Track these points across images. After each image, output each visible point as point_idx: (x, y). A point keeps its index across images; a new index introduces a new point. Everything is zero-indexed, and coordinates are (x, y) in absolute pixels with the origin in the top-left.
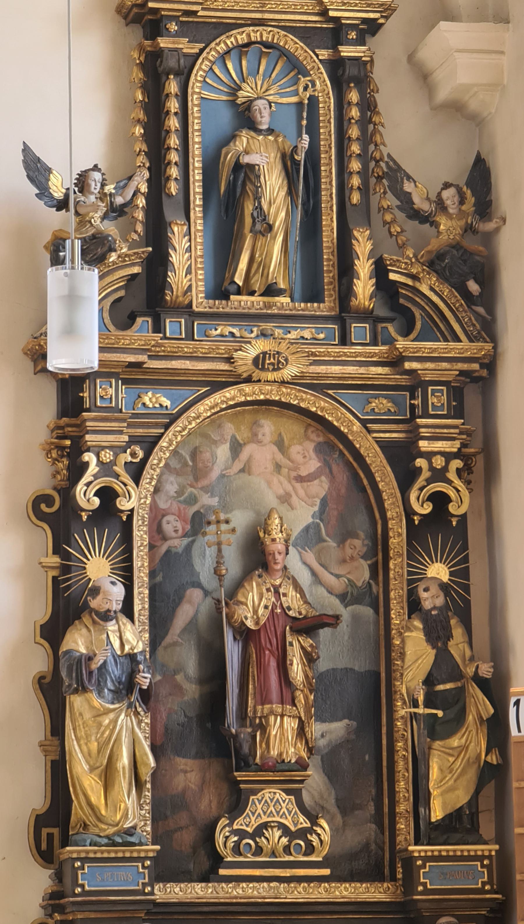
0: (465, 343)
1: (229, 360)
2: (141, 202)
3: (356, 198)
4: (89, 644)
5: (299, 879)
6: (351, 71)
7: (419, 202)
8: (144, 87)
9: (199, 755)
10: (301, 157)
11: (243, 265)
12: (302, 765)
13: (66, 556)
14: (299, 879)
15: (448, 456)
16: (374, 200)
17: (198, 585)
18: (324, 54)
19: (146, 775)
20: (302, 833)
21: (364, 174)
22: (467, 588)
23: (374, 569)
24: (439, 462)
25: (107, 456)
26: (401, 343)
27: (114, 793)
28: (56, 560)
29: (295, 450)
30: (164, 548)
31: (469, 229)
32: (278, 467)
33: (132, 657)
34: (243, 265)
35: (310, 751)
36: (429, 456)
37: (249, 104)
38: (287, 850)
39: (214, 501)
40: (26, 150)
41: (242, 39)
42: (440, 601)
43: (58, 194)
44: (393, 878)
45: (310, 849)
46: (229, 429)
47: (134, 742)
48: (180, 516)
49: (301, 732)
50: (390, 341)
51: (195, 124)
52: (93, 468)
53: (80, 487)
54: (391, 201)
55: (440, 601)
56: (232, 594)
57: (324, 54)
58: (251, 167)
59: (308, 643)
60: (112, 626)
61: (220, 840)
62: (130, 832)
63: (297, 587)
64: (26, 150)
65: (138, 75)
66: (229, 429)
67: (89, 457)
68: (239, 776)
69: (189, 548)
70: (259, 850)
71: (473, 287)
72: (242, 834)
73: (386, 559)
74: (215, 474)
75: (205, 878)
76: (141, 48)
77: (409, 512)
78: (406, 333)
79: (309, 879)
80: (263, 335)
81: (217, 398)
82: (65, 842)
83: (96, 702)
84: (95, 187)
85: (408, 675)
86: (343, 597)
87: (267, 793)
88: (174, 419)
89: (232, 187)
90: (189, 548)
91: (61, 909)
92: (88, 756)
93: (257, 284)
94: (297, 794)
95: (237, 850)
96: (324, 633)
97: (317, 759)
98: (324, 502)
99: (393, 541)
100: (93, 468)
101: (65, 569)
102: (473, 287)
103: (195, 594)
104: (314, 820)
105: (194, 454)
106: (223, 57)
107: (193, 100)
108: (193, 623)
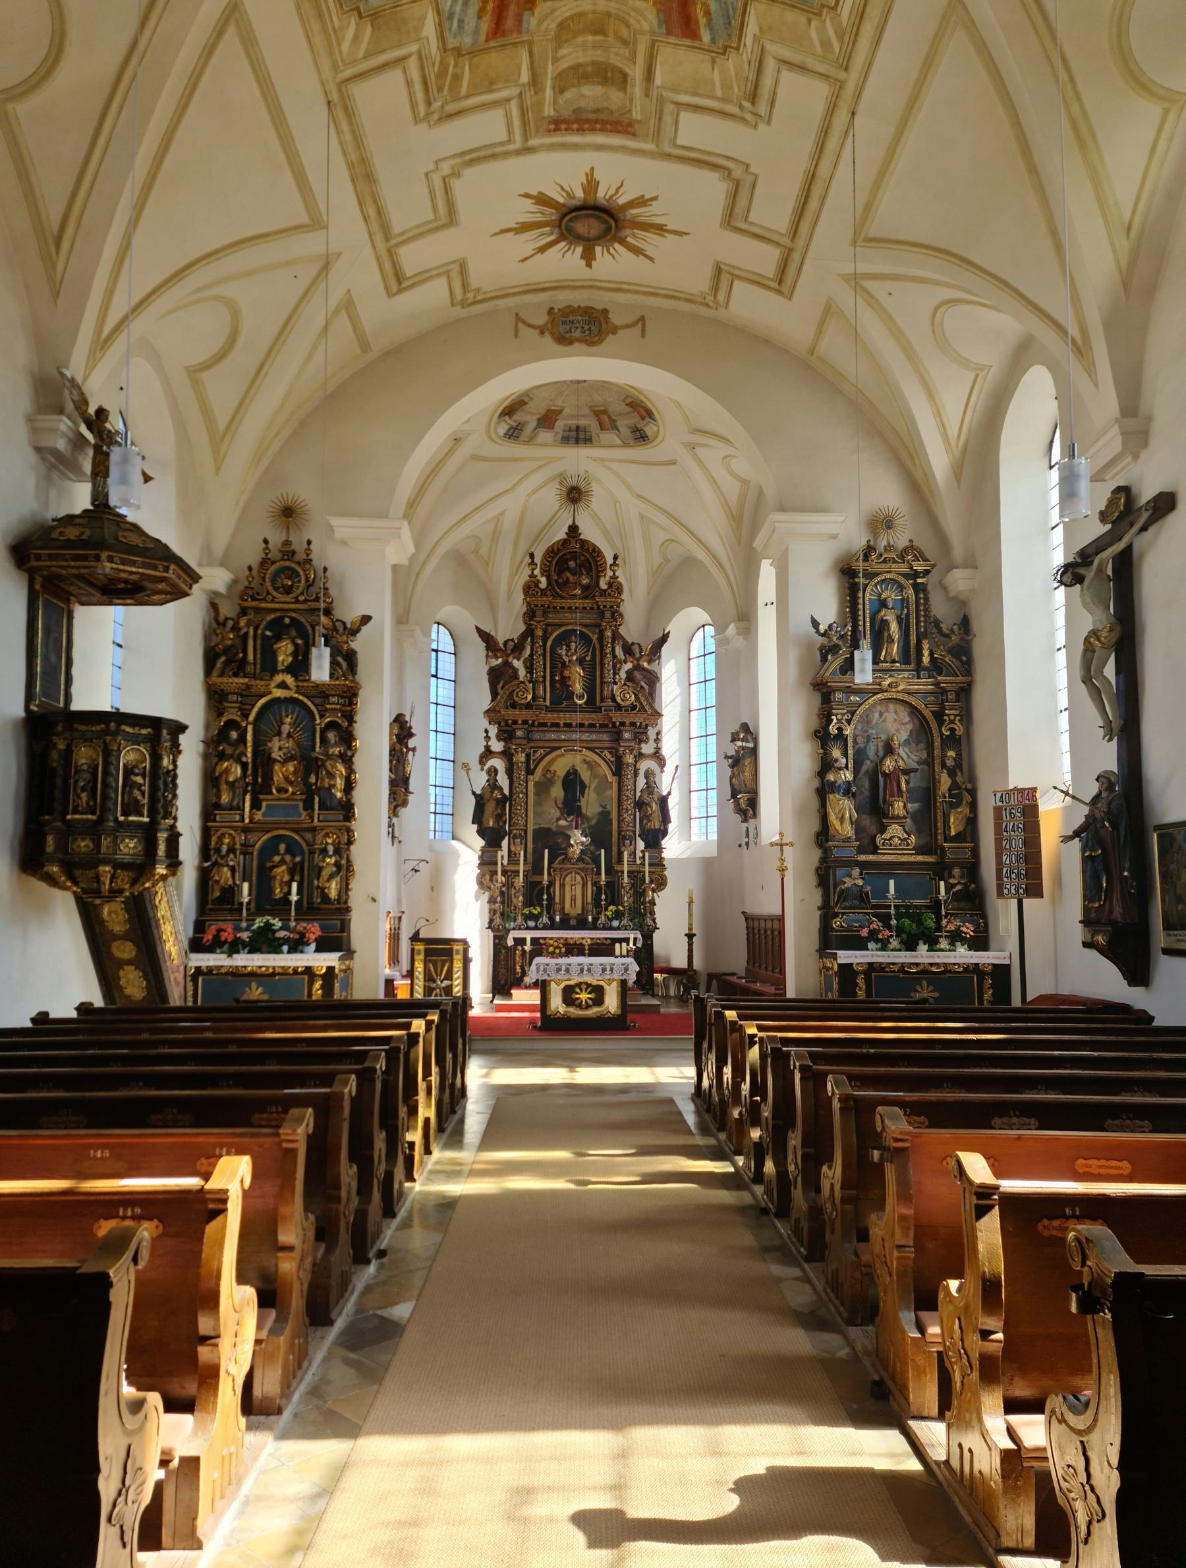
0: (961, 678)
1: (880, 685)
2: (849, 633)
3: (922, 630)
4: (835, 778)
5: (904, 854)
6: (921, 587)
7: (945, 630)
8: (850, 595)
9: (870, 814)
10: (903, 616)
11: (883, 653)
12: (905, 817)
13: (825, 750)
14: (904, 854)
15: (956, 716)
16: (929, 630)
17: (868, 759)
18: (911, 582)
19: (854, 820)
20: (905, 839)
21: (925, 622)
22: (961, 759)
23: (928, 753)
24: (952, 717)
25: (840, 717)
26: (939, 678)
27: (844, 825)
28: (822, 751)
29: (901, 714)
30: (857, 747)
31: (962, 639)
32: (895, 720)
33: (849, 782)
34: (883, 653)
35: (907, 813)
36: (949, 715)
37: (885, 599)
38: (900, 845)
39: (874, 732)
40: (812, 617)
41: (883, 578)
42: (953, 764)
43: (822, 631)
44: (936, 854)
45: (908, 845)
46: (879, 708)
47: (850, 809)
48: (863, 737)
49: (905, 807)
50: (936, 678)
51: (867, 607)
52: (835, 721)
53: (831, 727)
54: (934, 630)
55: (953, 764)
56: (881, 761)
57: (911, 582)
58: (887, 620)
59: (907, 777)
60: (842, 772)
61: (878, 841)
62: (850, 838)
63: (903, 760)
64: (812, 617)
65: (847, 592)
66: (879, 708)
67: (834, 717)
68: (884, 820)
69: (865, 747)
70: (891, 845)
71: (964, 659)
72: (885, 839)
73: (933, 750)
74: (874, 722)
75: (873, 853)
76: (849, 583)
77: (941, 734)
78: (940, 675)
79: (908, 854)
80: (891, 676)
81: (875, 697)
82: (827, 841)
83: (838, 796)
84: (834, 629)
85: (942, 788)
86: (918, 763)
87: (893, 826)
88: (861, 704)
89: (880, 627)
90: (865, 747)
91: (826, 862)
92: (835, 814)
93: (888, 659)
94: (903, 826)
95: (883, 845)
96: (912, 774)
97: (909, 816)
98: (911, 731)
99: (936, 744)
100: (835, 721)
101: (825, 754)
102: (964, 659)
103: (868, 762)
104: (909, 835)
105: (867, 716)
106: (876, 585)
107: (867, 599)
108: (867, 772)
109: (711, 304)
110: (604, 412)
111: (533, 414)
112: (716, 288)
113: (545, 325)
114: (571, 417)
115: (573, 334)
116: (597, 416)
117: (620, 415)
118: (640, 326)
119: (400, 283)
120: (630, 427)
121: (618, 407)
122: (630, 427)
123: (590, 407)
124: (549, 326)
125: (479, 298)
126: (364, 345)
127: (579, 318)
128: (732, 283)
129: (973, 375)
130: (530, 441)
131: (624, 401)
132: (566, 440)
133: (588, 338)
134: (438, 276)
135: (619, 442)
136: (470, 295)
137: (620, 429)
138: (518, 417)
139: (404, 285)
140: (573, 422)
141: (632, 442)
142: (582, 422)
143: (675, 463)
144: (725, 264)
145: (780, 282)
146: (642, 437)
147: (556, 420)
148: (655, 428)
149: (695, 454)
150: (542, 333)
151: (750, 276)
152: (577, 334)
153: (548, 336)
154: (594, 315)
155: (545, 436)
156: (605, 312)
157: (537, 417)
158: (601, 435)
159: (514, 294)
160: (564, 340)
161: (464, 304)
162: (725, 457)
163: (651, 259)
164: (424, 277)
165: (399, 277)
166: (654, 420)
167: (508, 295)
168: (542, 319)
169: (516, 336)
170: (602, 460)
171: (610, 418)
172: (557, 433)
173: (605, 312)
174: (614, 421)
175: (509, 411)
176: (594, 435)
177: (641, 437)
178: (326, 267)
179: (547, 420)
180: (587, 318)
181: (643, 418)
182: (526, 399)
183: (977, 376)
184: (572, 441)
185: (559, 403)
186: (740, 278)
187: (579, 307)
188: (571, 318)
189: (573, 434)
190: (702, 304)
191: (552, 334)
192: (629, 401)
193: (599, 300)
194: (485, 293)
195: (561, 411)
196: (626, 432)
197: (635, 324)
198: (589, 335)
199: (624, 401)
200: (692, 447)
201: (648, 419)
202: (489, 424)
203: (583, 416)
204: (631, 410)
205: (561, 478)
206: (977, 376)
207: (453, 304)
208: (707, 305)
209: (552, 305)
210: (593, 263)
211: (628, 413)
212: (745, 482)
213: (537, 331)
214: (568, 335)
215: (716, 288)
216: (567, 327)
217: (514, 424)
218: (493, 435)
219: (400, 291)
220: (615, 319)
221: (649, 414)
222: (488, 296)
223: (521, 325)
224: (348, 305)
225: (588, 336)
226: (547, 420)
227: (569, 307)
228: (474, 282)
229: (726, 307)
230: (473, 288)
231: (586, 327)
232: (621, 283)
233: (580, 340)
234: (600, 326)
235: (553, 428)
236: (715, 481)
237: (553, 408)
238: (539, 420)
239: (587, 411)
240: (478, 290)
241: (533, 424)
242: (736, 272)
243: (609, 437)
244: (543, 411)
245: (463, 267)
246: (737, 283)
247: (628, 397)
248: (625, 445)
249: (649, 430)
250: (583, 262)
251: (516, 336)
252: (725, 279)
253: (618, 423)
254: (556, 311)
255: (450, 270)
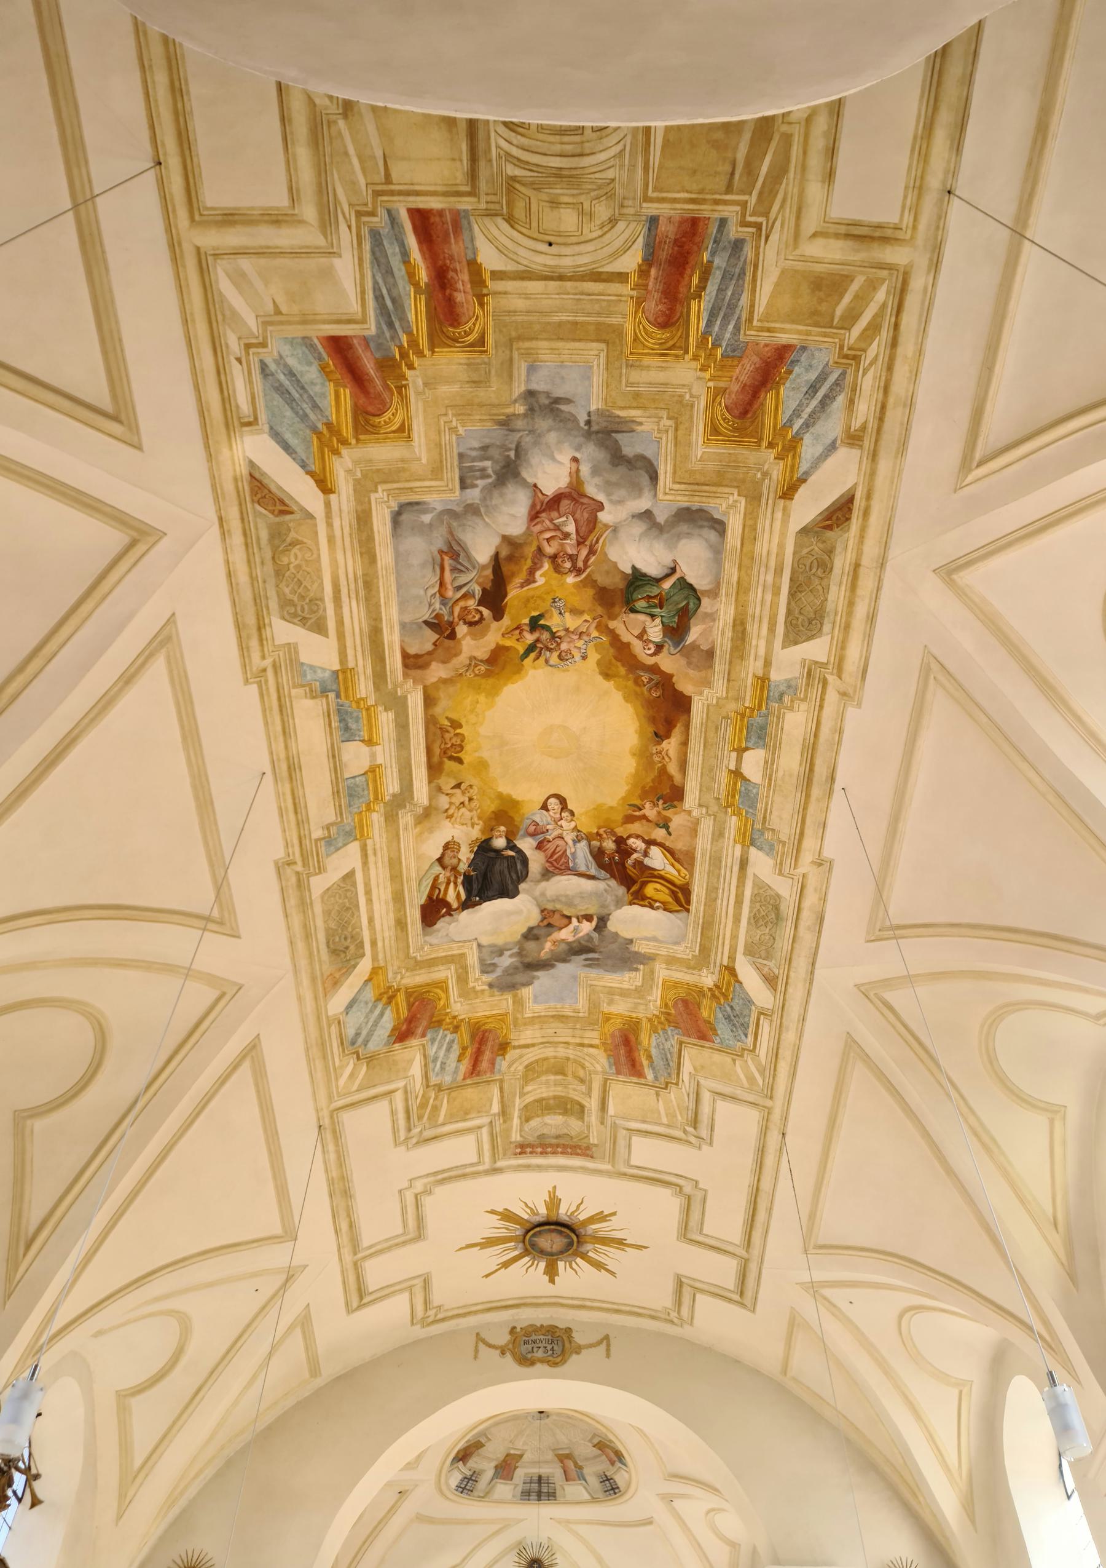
109: (676, 1320)
110: (569, 1456)
111: (490, 1460)
112: (679, 1303)
113: (507, 1345)
114: (534, 1463)
115: (535, 1354)
116: (562, 1462)
117: (587, 1459)
118: (604, 1346)
119: (361, 1298)
120: (599, 1476)
121: (584, 1450)
122: (599, 1476)
123: (554, 1450)
124: (511, 1346)
125: (440, 1316)
126: (314, 1370)
127: (542, 1337)
128: (694, 1295)
129: (956, 1392)
130: (485, 1496)
131: (590, 1441)
132: (526, 1495)
133: (551, 1358)
134: (401, 1291)
135: (587, 1497)
136: (431, 1313)
137: (588, 1478)
138: (474, 1463)
139: (365, 1301)
140: (535, 1471)
141: (601, 1495)
142: (545, 1471)
143: (651, 1523)
144: (686, 1277)
145: (742, 1294)
146: (613, 1489)
147: (516, 1468)
148: (626, 1475)
149: (674, 1509)
150: (503, 1353)
151: (712, 1289)
152: (540, 1354)
153: (509, 1357)
154: (557, 1334)
155: (504, 1489)
156: (569, 1330)
157: (493, 1464)
158: (566, 1487)
159: (476, 1312)
160: (525, 1361)
161: (425, 1323)
162: (708, 1512)
163: (612, 1273)
164: (387, 1292)
165: (361, 1293)
166: (626, 1466)
167: (469, 1313)
168: (503, 1338)
169: (476, 1358)
170: (568, 1522)
171: (576, 1464)
172: (516, 1485)
173: (569, 1330)
174: (581, 1468)
175: (463, 1456)
176: (558, 1487)
177: (611, 1488)
178: (290, 1278)
179: (506, 1468)
180: (550, 1337)
181: (613, 1463)
182: (483, 1440)
183: (961, 1392)
184: (534, 1496)
185: (519, 1445)
186: (702, 1291)
187: (542, 1326)
188: (534, 1337)
189: (535, 1486)
190: (666, 1320)
191: (513, 1355)
192: (596, 1441)
193: (561, 1318)
194: (447, 1310)
195: (521, 1456)
196: (594, 1481)
197: (600, 1343)
198: (551, 1355)
199: (590, 1441)
200: (669, 1499)
201: (618, 1464)
202: (441, 1471)
203: (547, 1462)
204: (599, 1452)
205: (520, 1548)
206: (961, 1392)
207: (412, 1324)
208: (672, 1322)
209: (514, 1325)
210: (556, 1278)
211: (596, 1457)
212: (733, 1545)
213: (498, 1352)
214: (529, 1356)
215: (679, 1303)
216: (529, 1347)
217: (469, 1473)
218: (444, 1488)
219: (360, 1307)
220: (579, 1338)
221: (619, 1456)
222: (450, 1314)
223: (481, 1346)
224: (305, 1322)
225: (551, 1355)
226: (506, 1468)
227: (532, 1326)
228: (437, 1299)
229: (691, 1324)
230: (435, 1304)
231: (549, 1347)
232: (584, 1299)
233: (542, 1361)
234: (564, 1346)
235: (512, 1479)
236: (699, 1545)
237: (512, 1452)
238: (496, 1467)
239: (550, 1456)
240: (440, 1307)
241: (490, 1473)
242: (698, 1285)
243: (574, 1490)
244: (501, 1456)
245: (427, 1282)
246: (698, 1296)
247: (595, 1435)
248: (594, 1500)
249: (620, 1479)
250: (546, 1278)
251: (476, 1358)
252: (686, 1291)
253: (586, 1471)
254: (518, 1330)
255: (414, 1286)
